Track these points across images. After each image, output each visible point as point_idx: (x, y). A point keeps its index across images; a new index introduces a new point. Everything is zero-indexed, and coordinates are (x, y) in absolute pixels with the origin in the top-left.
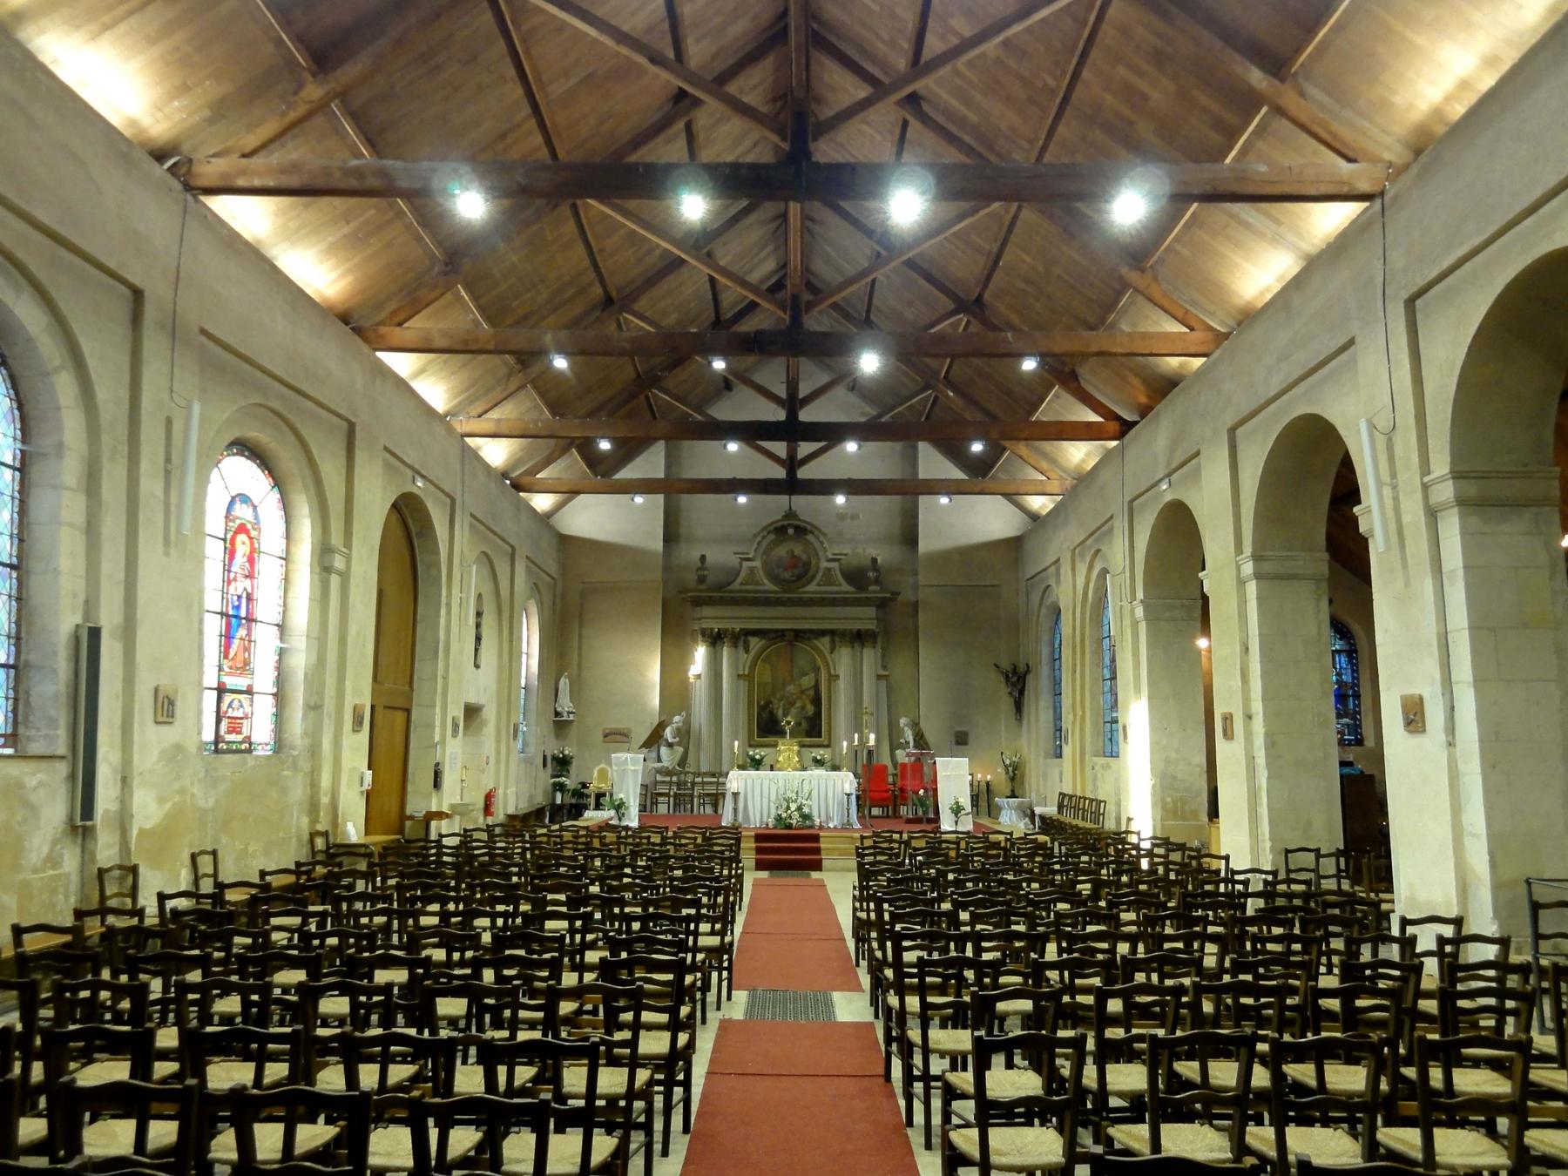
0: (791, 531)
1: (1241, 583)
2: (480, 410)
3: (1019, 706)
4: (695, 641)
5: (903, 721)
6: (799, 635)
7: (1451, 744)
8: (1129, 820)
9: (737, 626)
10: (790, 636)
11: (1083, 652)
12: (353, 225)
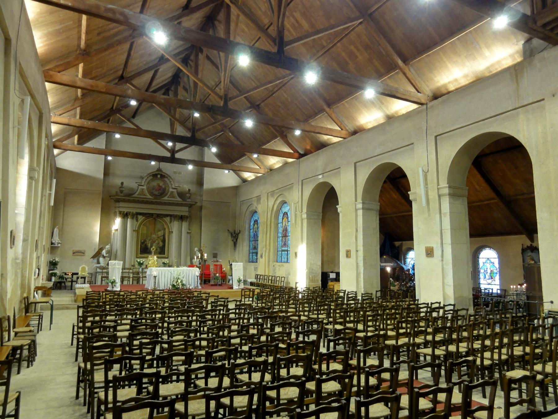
0: (159, 176)
1: (356, 210)
2: (61, 113)
3: (235, 244)
4: (115, 216)
5: (196, 249)
6: (159, 216)
7: (442, 260)
8: (296, 283)
9: (135, 211)
11: (271, 228)
12: (61, 26)
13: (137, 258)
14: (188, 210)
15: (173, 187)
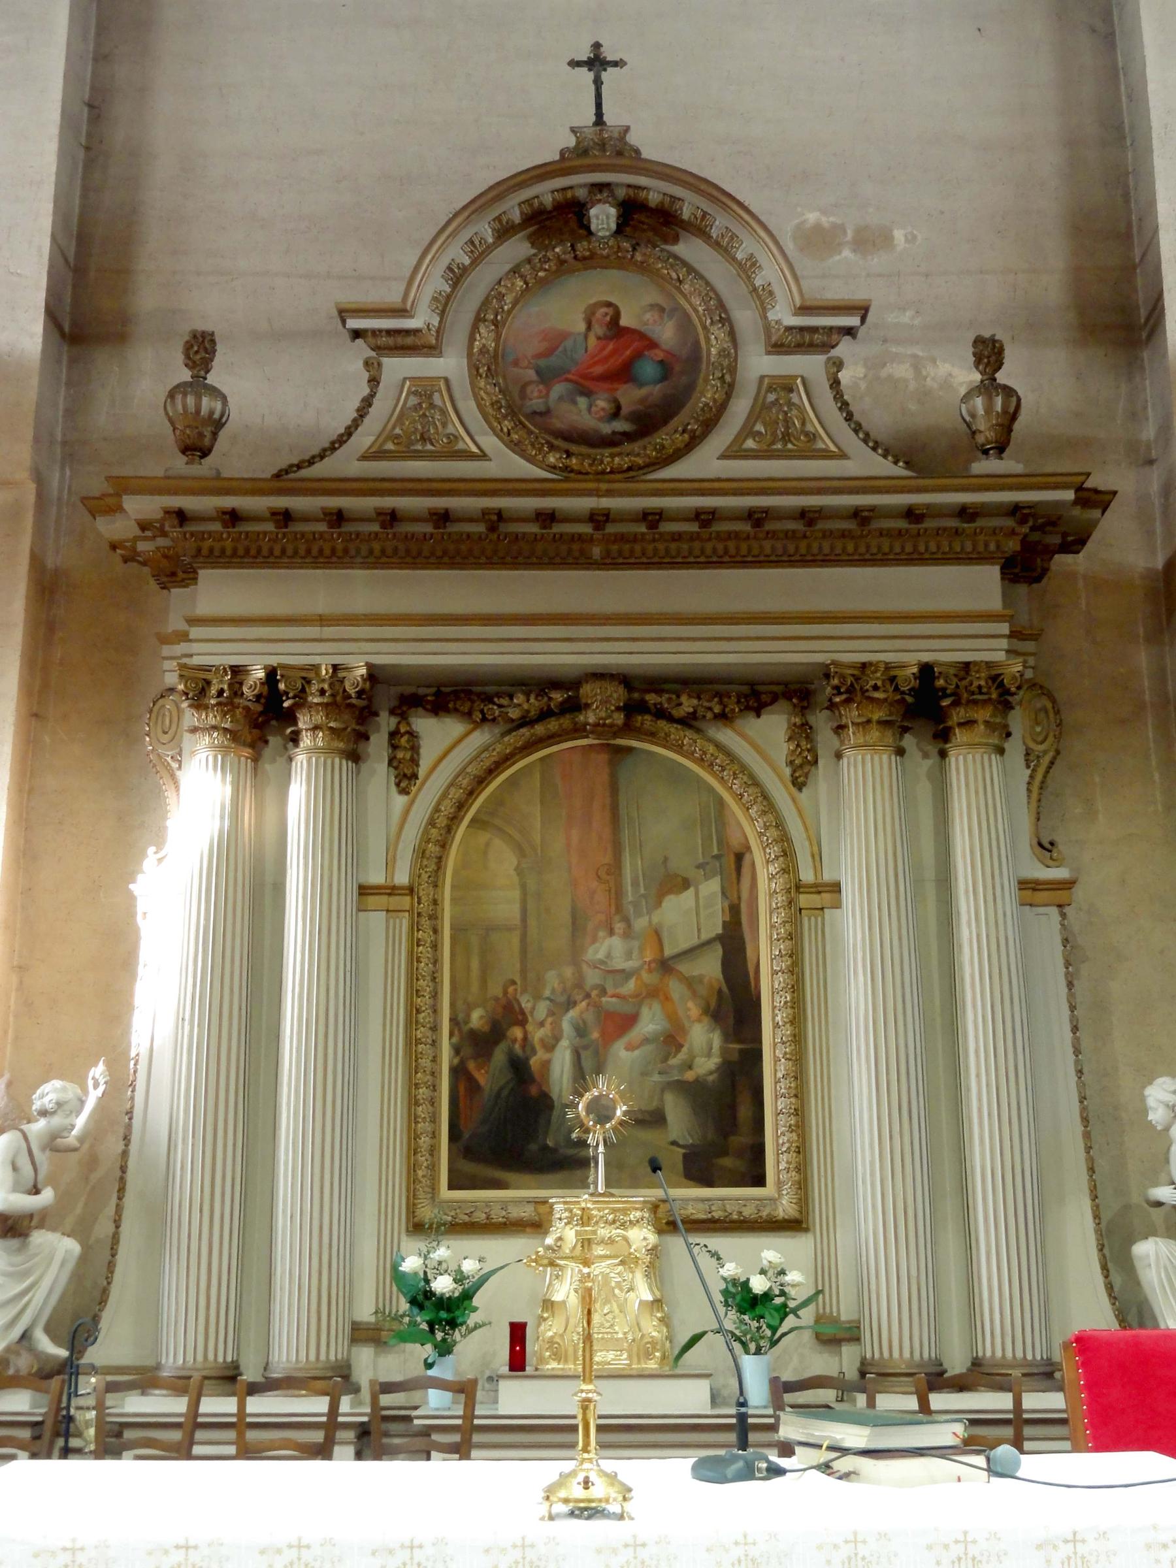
0: (603, 217)
6: (651, 702)
10: (601, 705)
13: (417, 1228)
14: (995, 603)
15: (783, 315)
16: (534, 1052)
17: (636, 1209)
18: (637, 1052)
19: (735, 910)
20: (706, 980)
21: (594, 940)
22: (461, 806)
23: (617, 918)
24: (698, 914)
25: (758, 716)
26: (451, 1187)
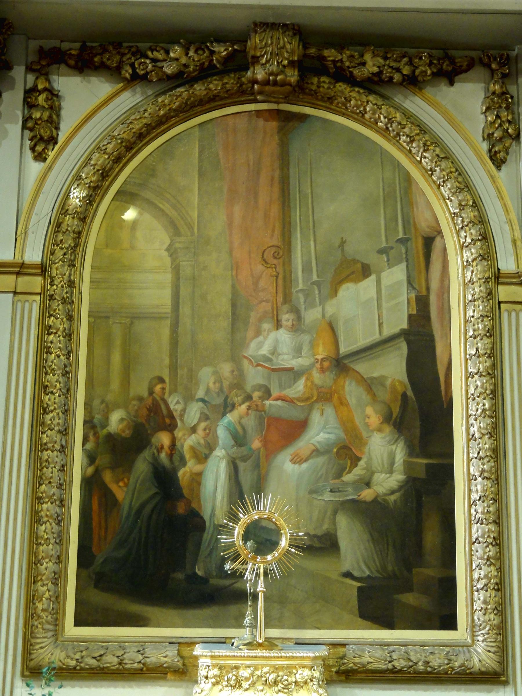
16: (183, 462)
17: (304, 667)
18: (305, 466)
19: (422, 303)
20: (388, 383)
21: (258, 333)
22: (106, 175)
23: (285, 308)
24: (379, 306)
25: (452, 83)
26: (78, 623)
